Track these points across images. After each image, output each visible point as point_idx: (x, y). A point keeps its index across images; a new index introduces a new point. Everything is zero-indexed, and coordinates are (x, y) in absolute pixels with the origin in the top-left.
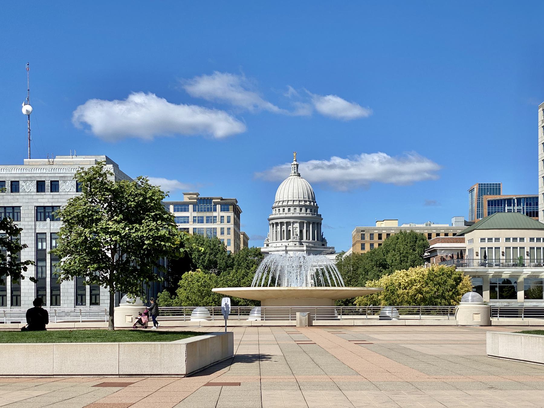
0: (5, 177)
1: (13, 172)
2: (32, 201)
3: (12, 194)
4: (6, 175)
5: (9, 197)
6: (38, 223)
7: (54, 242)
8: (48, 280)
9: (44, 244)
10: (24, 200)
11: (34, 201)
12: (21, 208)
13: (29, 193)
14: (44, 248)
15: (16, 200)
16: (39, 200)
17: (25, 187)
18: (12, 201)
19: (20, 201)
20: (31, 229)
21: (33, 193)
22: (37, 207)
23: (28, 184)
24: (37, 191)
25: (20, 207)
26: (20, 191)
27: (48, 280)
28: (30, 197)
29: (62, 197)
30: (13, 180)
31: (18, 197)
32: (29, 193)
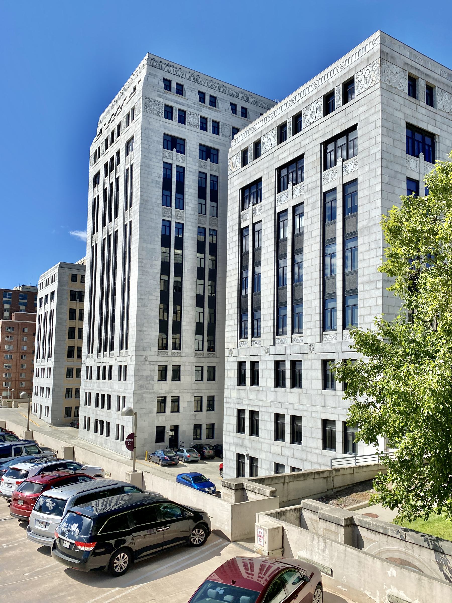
29: (305, 136)
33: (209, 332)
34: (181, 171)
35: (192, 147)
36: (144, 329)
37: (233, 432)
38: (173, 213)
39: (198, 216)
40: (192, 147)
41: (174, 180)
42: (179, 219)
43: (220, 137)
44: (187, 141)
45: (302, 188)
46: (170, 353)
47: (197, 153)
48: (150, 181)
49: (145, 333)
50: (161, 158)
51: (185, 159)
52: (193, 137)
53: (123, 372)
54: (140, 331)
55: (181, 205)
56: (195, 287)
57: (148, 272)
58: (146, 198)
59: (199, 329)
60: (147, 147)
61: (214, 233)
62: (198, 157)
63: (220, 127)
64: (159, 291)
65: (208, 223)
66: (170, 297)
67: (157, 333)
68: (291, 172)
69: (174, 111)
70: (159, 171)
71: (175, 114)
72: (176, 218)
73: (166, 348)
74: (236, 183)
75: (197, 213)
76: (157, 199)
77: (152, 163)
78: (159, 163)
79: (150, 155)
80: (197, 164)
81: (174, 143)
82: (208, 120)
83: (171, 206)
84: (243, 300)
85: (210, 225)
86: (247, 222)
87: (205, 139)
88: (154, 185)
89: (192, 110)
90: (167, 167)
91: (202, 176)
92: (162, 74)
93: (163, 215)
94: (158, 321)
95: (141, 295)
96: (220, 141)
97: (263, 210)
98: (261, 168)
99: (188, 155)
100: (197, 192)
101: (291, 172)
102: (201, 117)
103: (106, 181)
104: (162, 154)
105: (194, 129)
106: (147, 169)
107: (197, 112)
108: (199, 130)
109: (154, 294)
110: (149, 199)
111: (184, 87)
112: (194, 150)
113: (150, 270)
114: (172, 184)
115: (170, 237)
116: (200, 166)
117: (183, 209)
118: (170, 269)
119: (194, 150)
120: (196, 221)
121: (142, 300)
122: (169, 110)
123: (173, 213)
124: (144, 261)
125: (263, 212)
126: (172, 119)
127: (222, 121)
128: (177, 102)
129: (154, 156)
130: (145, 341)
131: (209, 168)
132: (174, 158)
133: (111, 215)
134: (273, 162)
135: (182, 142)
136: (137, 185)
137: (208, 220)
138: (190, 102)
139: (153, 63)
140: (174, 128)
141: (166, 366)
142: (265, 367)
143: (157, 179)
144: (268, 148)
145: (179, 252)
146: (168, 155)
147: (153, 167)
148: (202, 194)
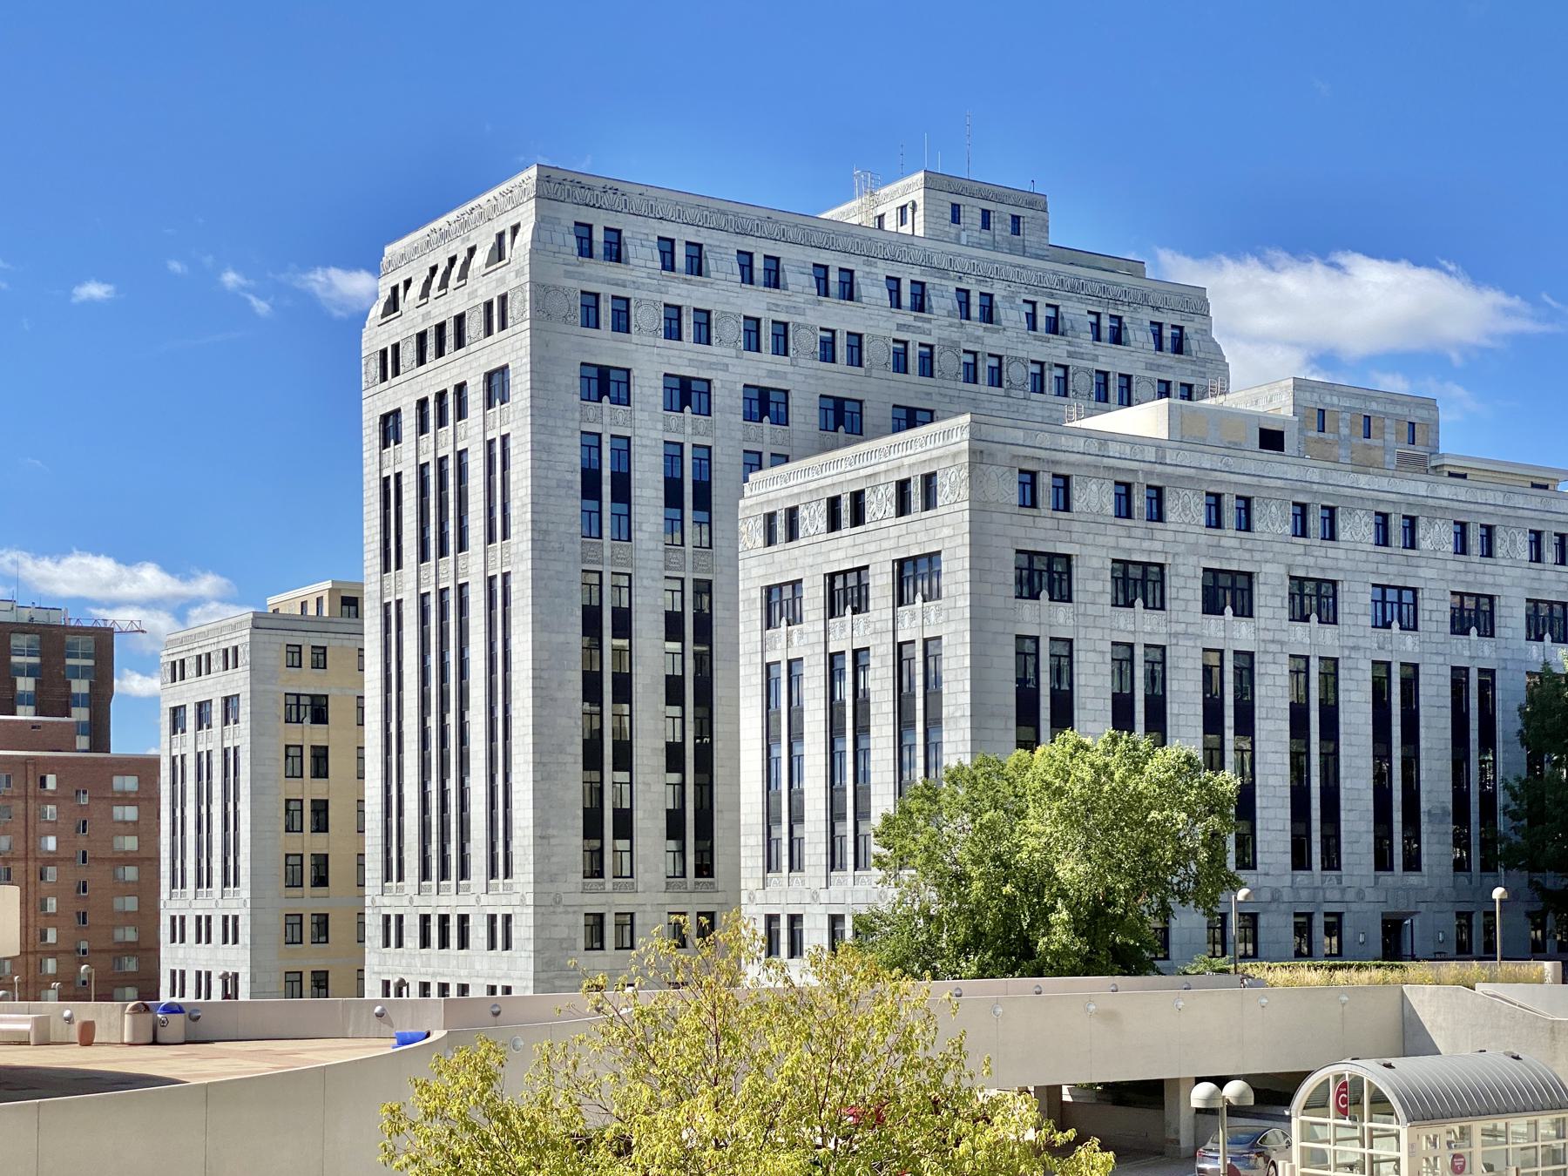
33: (697, 831)
34: (623, 449)
35: (648, 388)
36: (551, 831)
39: (666, 551)
40: (648, 388)
41: (606, 472)
42: (622, 565)
43: (714, 348)
44: (634, 373)
45: (867, 623)
46: (609, 886)
47: (659, 398)
48: (554, 483)
49: (553, 841)
50: (575, 425)
52: (650, 359)
53: (500, 932)
54: (542, 837)
55: (625, 532)
56: (661, 725)
57: (553, 700)
58: (544, 527)
59: (674, 827)
60: (543, 403)
61: (704, 588)
62: (660, 409)
63: (713, 324)
64: (579, 741)
65: (689, 566)
66: (604, 753)
67: (579, 840)
68: (846, 592)
69: (602, 304)
70: (571, 460)
71: (606, 310)
73: (601, 875)
74: (754, 572)
75: (661, 547)
76: (571, 525)
77: (555, 440)
78: (572, 437)
79: (551, 423)
80: (660, 426)
81: (606, 383)
82: (684, 311)
83: (600, 537)
84: (772, 799)
86: (777, 654)
87: (679, 361)
88: (562, 492)
89: (643, 294)
90: (591, 442)
91: (673, 454)
92: (570, 214)
93: (584, 561)
94: (580, 813)
95: (541, 754)
96: (714, 359)
97: (804, 641)
98: (800, 561)
99: (638, 406)
100: (662, 494)
101: (846, 592)
102: (666, 305)
103: (423, 445)
104: (577, 415)
105: (651, 340)
106: (544, 457)
107: (657, 297)
108: (662, 342)
109: (569, 749)
110: (551, 527)
111: (624, 234)
112: (652, 391)
113: (559, 695)
114: (602, 483)
115: (604, 621)
116: (667, 430)
117: (629, 540)
118: (603, 686)
119: (652, 391)
120: (661, 565)
121: (544, 765)
122: (591, 301)
123: (607, 552)
124: (545, 675)
125: (808, 639)
126: (597, 326)
127: (719, 307)
128: (608, 282)
129: (559, 423)
130: (554, 859)
131: (689, 430)
132: (606, 419)
133: (443, 540)
134: (820, 559)
135: (622, 376)
136: (522, 492)
138: (640, 275)
139: (551, 190)
140: (606, 348)
141: (601, 916)
143: (569, 477)
144: (812, 531)
145: (625, 643)
146: (591, 415)
147: (558, 449)
148: (673, 496)
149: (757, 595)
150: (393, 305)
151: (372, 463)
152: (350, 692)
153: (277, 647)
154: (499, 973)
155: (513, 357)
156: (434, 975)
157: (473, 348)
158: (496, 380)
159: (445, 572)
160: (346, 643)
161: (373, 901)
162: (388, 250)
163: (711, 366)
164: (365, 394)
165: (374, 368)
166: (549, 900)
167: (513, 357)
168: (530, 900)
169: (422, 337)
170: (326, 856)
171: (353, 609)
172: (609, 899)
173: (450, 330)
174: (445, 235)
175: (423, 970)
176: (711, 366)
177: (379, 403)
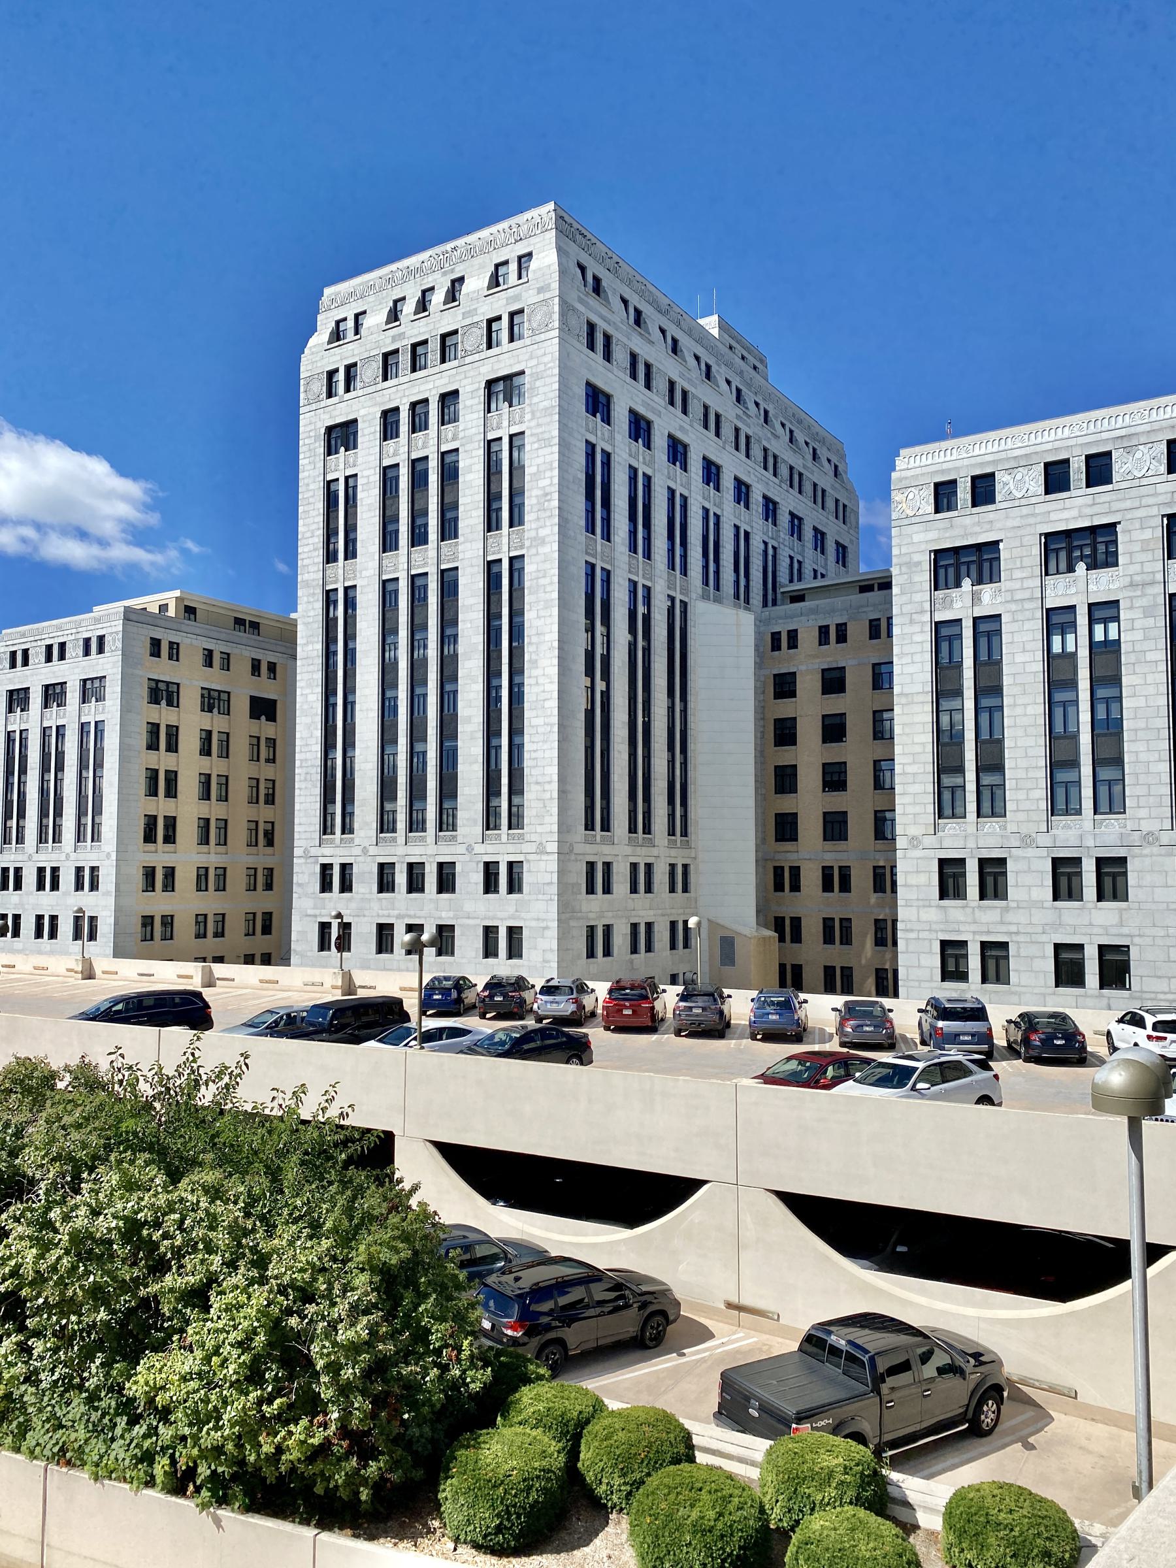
0: (957, 469)
1: (977, 452)
2: (1032, 520)
3: (976, 510)
4: (958, 464)
5: (968, 521)
6: (1050, 580)
7: (1099, 629)
8: (1085, 739)
9: (1070, 638)
10: (1010, 523)
11: (1039, 519)
12: (1001, 546)
13: (1024, 502)
14: (1070, 648)
15: (987, 527)
16: (1053, 516)
17: (1012, 486)
18: (977, 529)
19: (998, 525)
20: (1031, 599)
21: (1033, 500)
22: (1047, 535)
23: (1019, 477)
24: (1047, 493)
25: (997, 543)
26: (998, 498)
27: (1085, 739)
28: (1025, 510)
30: (978, 472)
31: (992, 516)
32: (1024, 502)
37: (931, 980)
38: (599, 548)
44: (615, 399)
51: (612, 438)
72: (602, 560)
85: (644, 577)
90: (591, 448)
105: (621, 375)
137: (641, 566)
142: (1026, 868)
149: (925, 562)
150: (422, 305)
151: (313, 470)
152: (196, 683)
153: (143, 638)
154: (500, 915)
155: (534, 362)
156: (398, 917)
157: (360, 392)
158: (419, 409)
159: (428, 560)
160: (194, 642)
161: (306, 851)
162: (328, 291)
163: (653, 411)
164: (302, 410)
165: (320, 386)
166: (566, 850)
167: (534, 362)
168: (553, 847)
169: (331, 374)
170: (175, 818)
171: (192, 616)
172: (599, 850)
173: (341, 376)
174: (412, 272)
175: (386, 912)
176: (653, 411)
177: (327, 416)
